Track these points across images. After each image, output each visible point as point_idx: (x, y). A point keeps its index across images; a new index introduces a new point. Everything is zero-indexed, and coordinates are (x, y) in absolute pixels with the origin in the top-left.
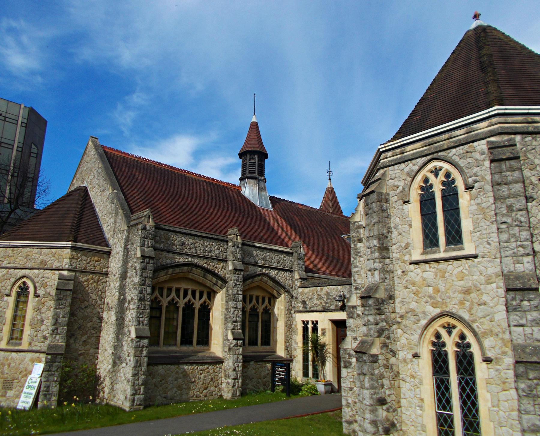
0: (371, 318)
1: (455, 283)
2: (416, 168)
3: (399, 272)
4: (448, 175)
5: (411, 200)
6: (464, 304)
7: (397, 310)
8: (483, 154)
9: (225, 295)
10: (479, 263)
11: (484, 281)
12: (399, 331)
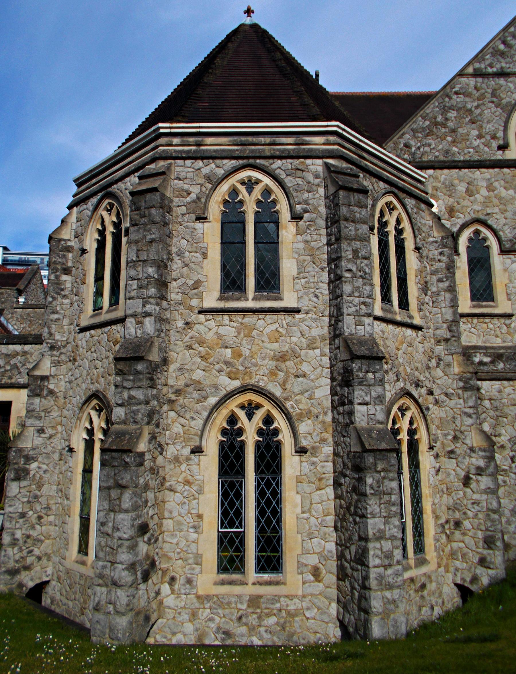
0: (139, 394)
1: (269, 346)
2: (221, 172)
3: (180, 324)
4: (267, 192)
5: (210, 218)
6: (276, 375)
7: (171, 382)
8: (317, 177)
10: (302, 320)
11: (305, 346)
12: (172, 414)
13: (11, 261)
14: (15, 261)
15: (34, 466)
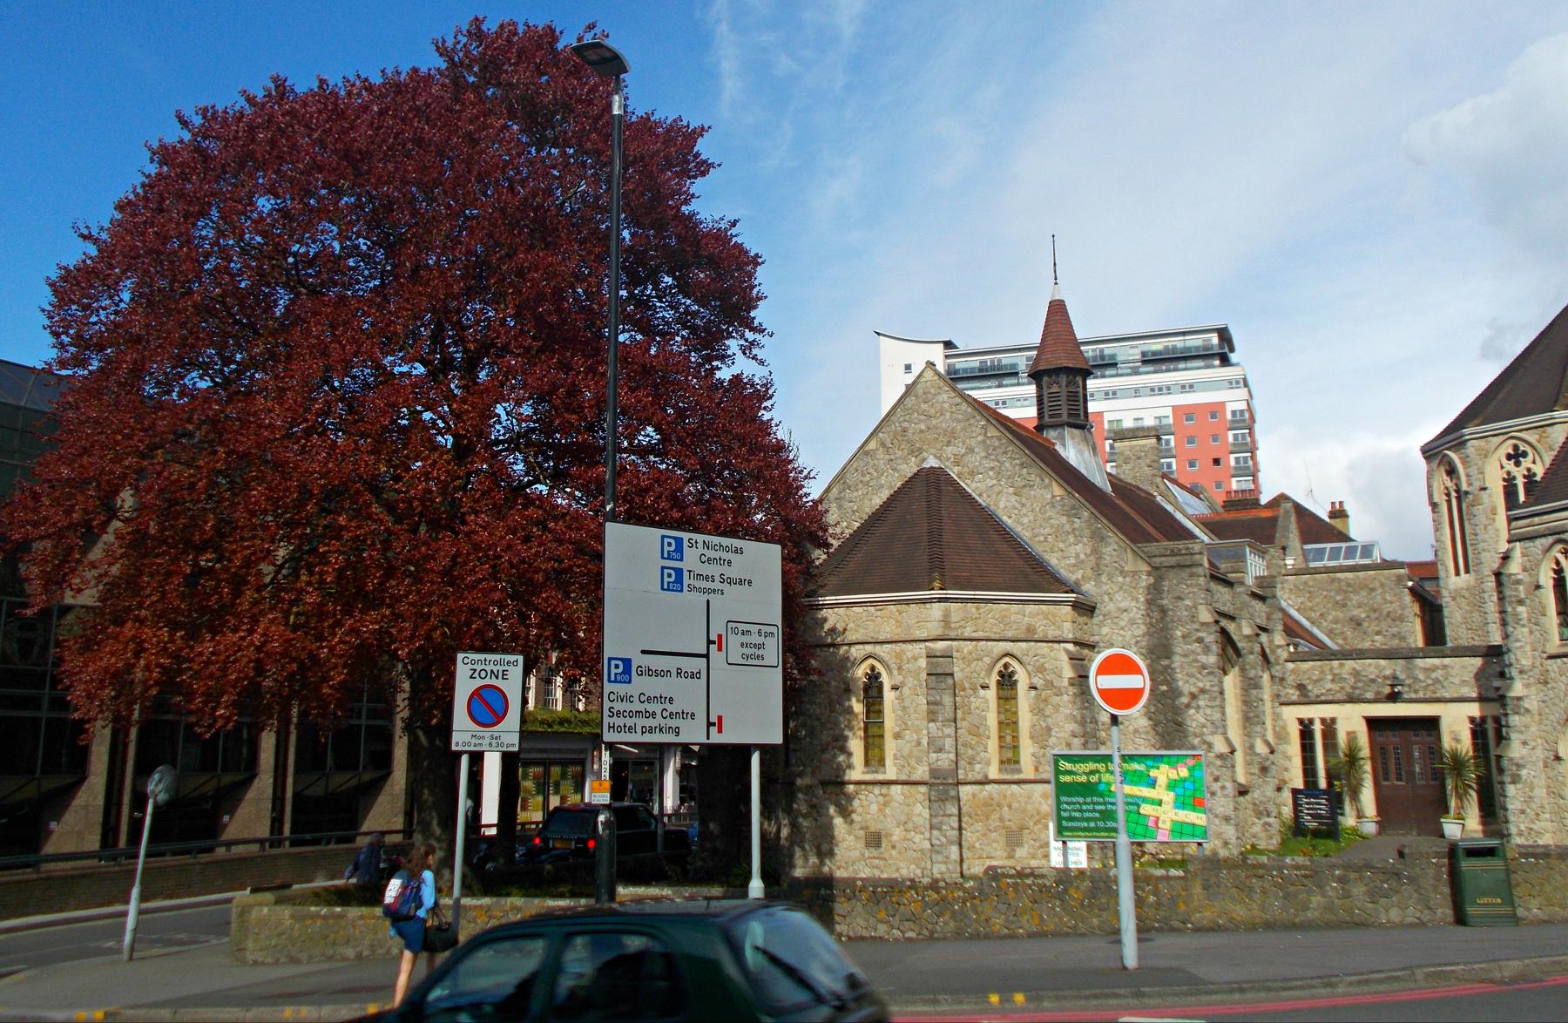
9: (1238, 679)
13: (965, 370)
14: (972, 370)
15: (1524, 772)
